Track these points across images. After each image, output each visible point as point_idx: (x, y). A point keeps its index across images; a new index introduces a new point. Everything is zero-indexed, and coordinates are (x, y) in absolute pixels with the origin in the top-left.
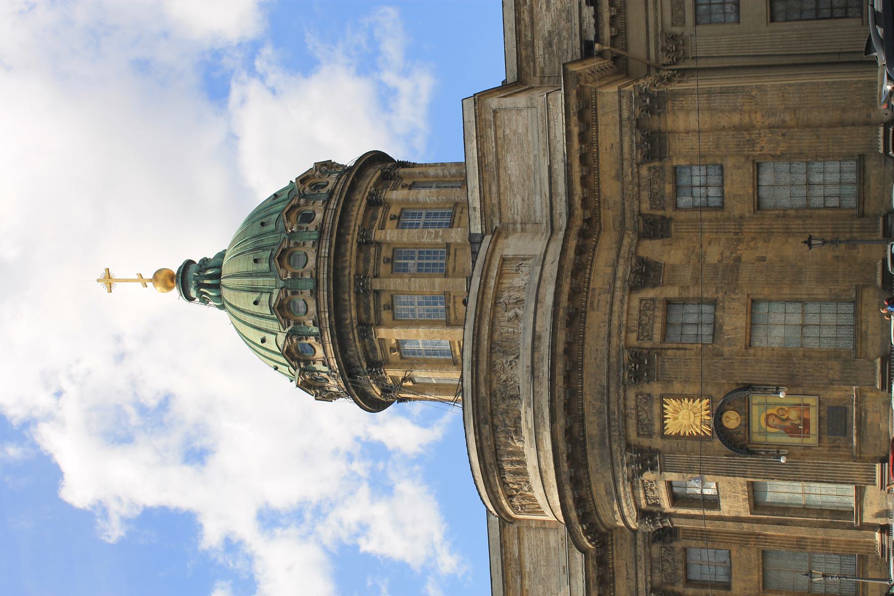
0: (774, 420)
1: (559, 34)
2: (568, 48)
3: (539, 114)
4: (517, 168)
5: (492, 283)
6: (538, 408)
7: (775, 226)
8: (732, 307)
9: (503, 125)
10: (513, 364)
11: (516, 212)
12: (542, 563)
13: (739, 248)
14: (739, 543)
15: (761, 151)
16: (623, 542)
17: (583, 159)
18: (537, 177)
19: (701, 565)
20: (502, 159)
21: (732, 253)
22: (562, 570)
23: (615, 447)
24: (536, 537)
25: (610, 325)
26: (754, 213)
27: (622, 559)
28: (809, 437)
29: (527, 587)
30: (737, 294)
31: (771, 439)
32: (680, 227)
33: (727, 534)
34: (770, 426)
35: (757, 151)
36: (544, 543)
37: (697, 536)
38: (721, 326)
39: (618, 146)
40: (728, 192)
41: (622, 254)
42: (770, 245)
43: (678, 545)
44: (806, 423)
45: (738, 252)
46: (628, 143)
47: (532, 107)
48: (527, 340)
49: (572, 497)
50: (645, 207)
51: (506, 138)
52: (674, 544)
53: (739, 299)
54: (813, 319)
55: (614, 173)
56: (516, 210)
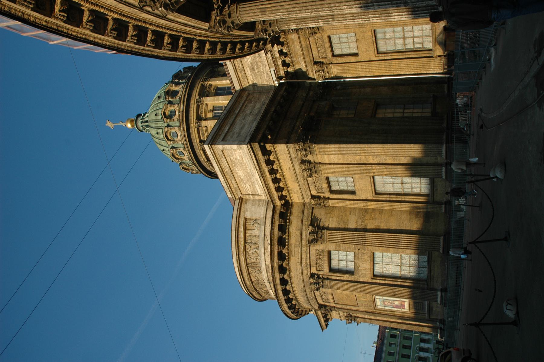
1: (257, 65)
2: (263, 71)
3: (246, 152)
5: (241, 235)
8: (363, 258)
13: (366, 218)
21: (362, 222)
25: (302, 265)
30: (365, 250)
41: (304, 223)
42: (383, 216)
45: (366, 221)
47: (241, 148)
48: (263, 267)
53: (366, 254)
55: (293, 179)
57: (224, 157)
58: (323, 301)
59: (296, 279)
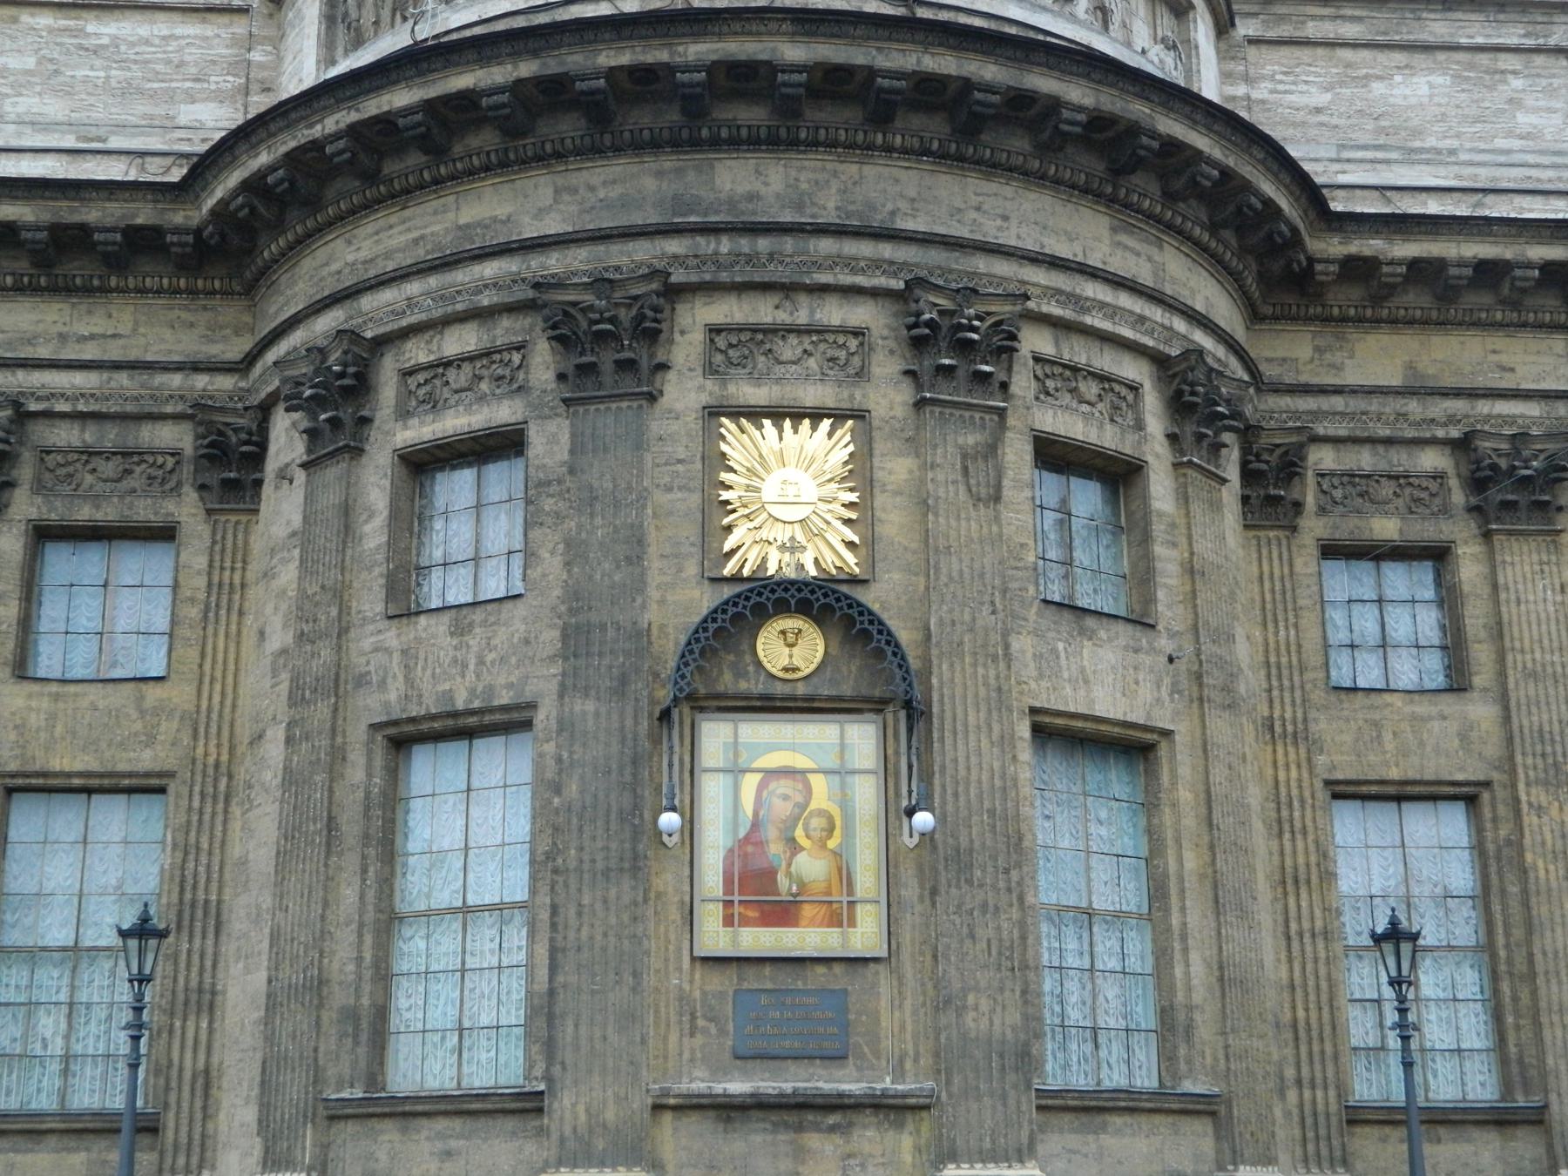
0: (786, 798)
4: (1413, 101)
7: (1300, 844)
8: (1141, 678)
9: (1534, 71)
11: (1281, 87)
14: (198, 706)
15: (1530, 804)
16: (200, 330)
17: (1488, 273)
19: (105, 586)
20: (1435, 62)
23: (674, 246)
24: (214, 62)
26: (1328, 783)
27: (136, 323)
28: (728, 921)
31: (713, 790)
32: (1275, 554)
33: (231, 667)
34: (762, 787)
35: (1528, 794)
36: (188, 84)
37: (222, 568)
39: (1507, 382)
40: (1388, 705)
43: (187, 509)
44: (782, 913)
46: (1522, 416)
49: (482, 85)
50: (1323, 458)
51: (1497, 77)
52: (190, 495)
54: (1106, 944)
56: (1287, 87)
57: (1530, 42)
58: (714, 330)
59: (975, 200)
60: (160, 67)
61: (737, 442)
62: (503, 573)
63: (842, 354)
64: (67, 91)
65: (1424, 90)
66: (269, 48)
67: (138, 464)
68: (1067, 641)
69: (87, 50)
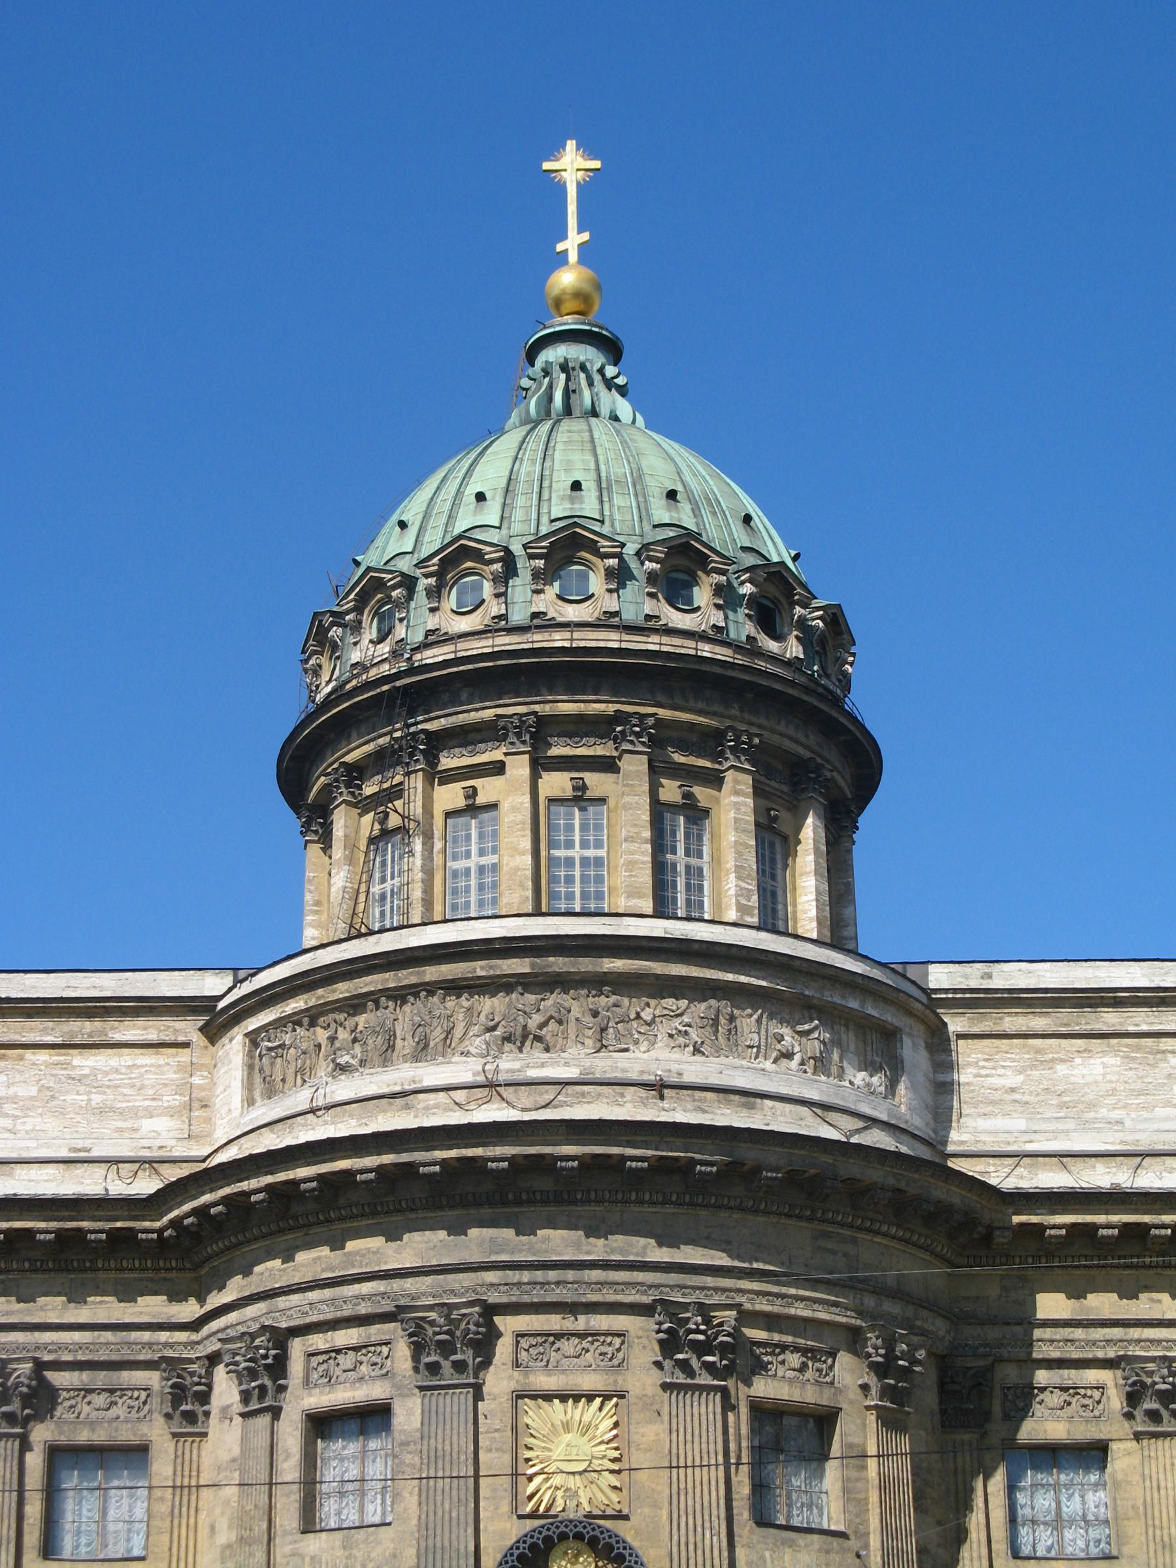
4: (1089, 1079)
6: (583, 1094)
10: (681, 1040)
11: (983, 1072)
12: (97, 1098)
18: (1071, 1125)
20: (1108, 1046)
22: (80, 1144)
23: (491, 1277)
24: (165, 1085)
29: (29, 1054)
38: (792, 1544)
51: (1159, 1056)
56: (988, 1072)
58: (520, 1335)
60: (125, 1091)
61: (534, 1415)
62: (379, 1501)
63: (610, 1350)
64: (61, 1112)
65: (1099, 1070)
66: (206, 1074)
67: (121, 1397)
68: (772, 1550)
69: (74, 1079)
